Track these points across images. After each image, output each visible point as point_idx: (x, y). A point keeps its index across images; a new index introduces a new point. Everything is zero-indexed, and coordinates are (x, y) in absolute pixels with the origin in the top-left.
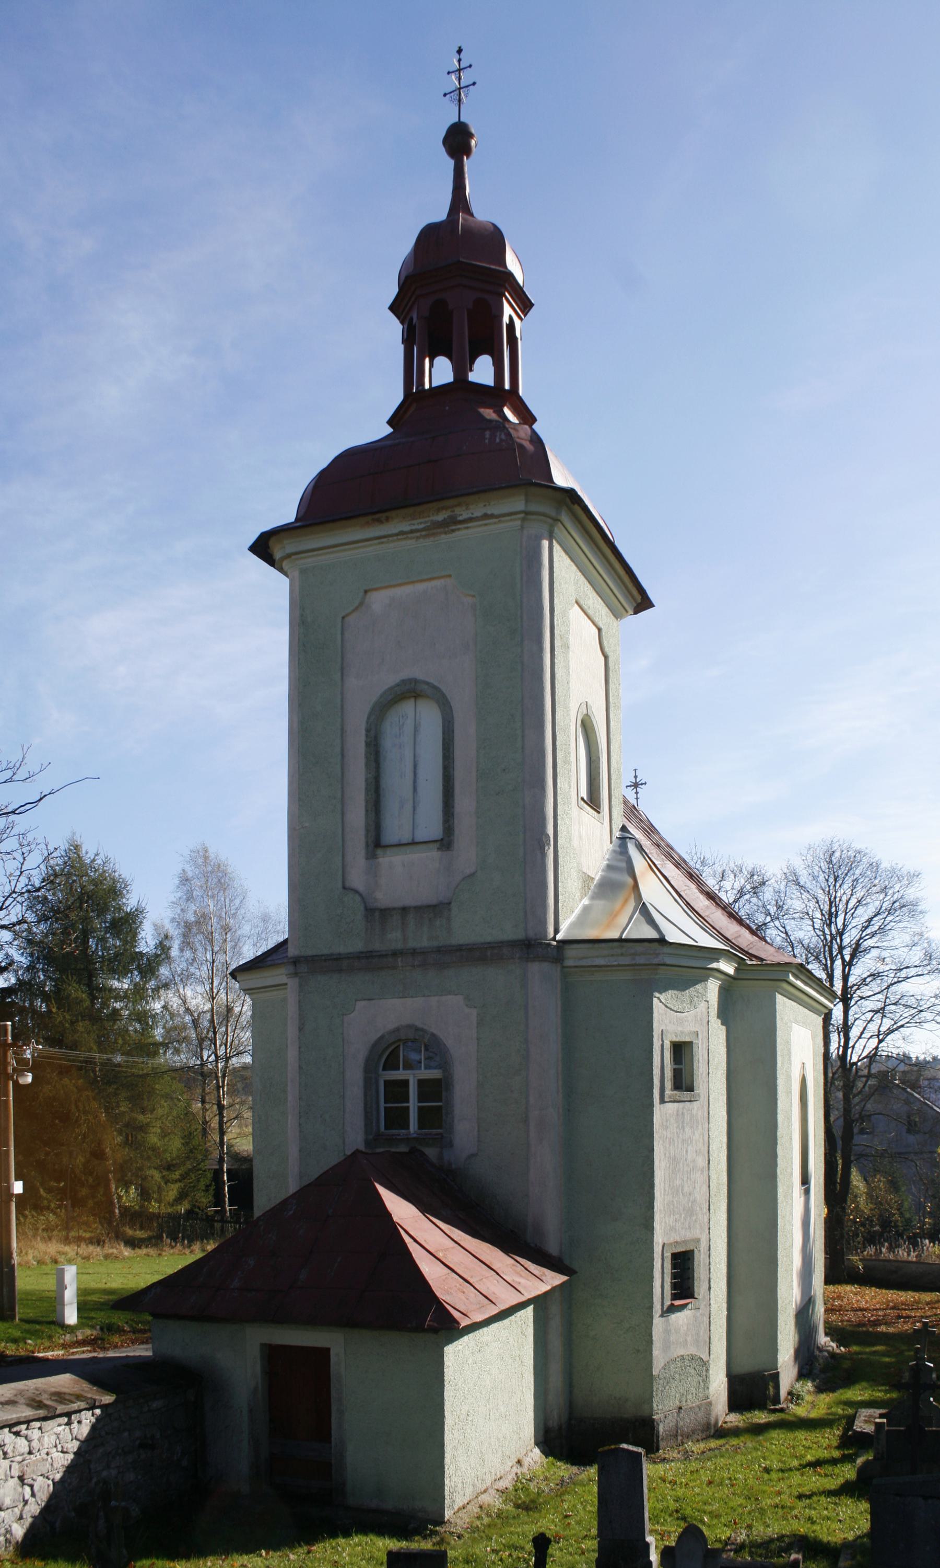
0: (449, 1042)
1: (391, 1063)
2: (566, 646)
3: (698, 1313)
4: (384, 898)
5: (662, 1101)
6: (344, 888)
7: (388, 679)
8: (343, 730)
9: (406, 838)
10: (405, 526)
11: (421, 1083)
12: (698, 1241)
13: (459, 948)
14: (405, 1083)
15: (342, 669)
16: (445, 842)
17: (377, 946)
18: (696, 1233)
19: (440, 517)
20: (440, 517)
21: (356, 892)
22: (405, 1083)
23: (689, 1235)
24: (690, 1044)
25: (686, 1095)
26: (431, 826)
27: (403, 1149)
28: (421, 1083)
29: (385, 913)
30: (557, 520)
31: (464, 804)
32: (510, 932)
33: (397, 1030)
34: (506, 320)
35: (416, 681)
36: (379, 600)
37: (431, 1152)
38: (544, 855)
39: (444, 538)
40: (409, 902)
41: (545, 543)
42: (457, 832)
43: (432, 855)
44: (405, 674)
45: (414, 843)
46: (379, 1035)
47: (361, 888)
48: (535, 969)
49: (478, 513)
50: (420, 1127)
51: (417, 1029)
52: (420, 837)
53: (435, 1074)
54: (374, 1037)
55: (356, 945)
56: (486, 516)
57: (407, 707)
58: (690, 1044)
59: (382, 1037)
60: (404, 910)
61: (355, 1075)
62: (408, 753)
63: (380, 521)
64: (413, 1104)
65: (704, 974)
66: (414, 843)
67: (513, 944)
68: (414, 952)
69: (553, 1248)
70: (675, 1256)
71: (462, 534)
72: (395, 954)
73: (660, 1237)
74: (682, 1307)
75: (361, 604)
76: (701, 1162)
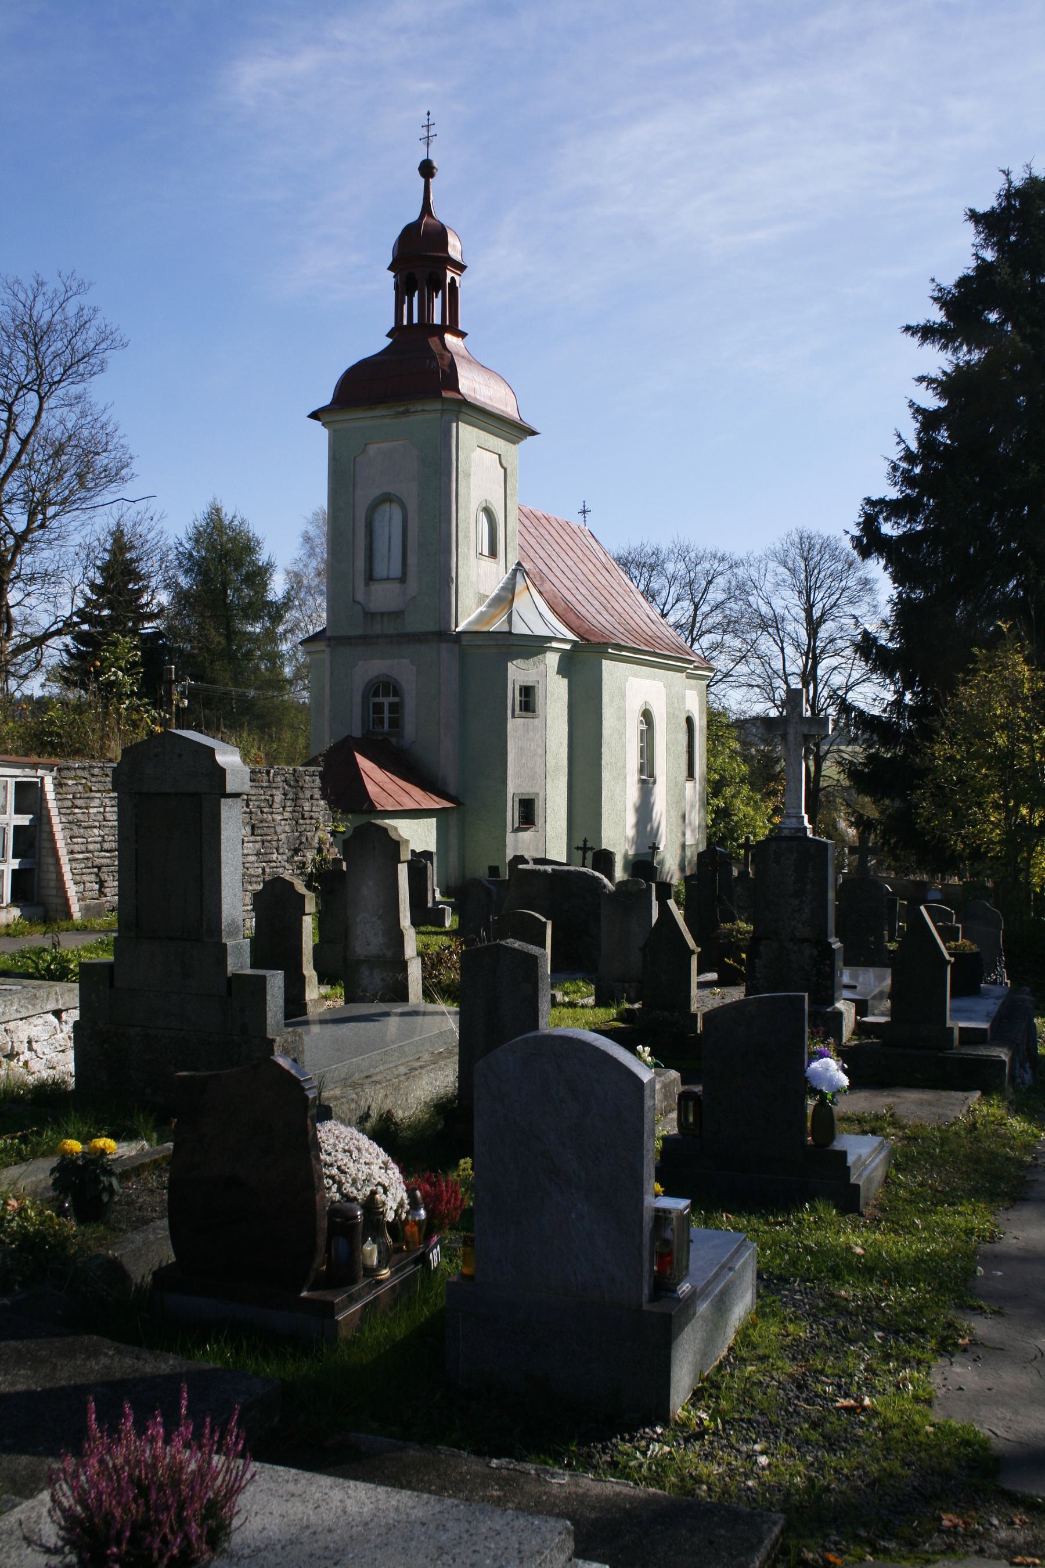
1: (376, 694)
2: (468, 475)
3: (538, 834)
4: (375, 606)
5: (513, 716)
6: (354, 601)
7: (377, 492)
8: (354, 518)
9: (385, 575)
10: (384, 412)
11: (391, 705)
12: (538, 794)
13: (408, 635)
15: (354, 485)
16: (403, 579)
18: (536, 790)
19: (401, 409)
20: (401, 409)
21: (359, 603)
23: (531, 791)
24: (533, 687)
25: (530, 714)
26: (396, 570)
27: (380, 738)
28: (391, 705)
29: (373, 615)
30: (460, 412)
31: (412, 560)
32: (432, 627)
33: (378, 676)
34: (448, 280)
35: (389, 494)
36: (372, 449)
37: (393, 740)
38: (450, 588)
39: (404, 420)
40: (384, 609)
41: (454, 425)
43: (395, 586)
44: (385, 490)
45: (388, 579)
48: (444, 646)
49: (420, 408)
50: (390, 727)
51: (388, 676)
52: (391, 576)
53: (396, 699)
55: (359, 632)
56: (423, 411)
57: (386, 507)
58: (533, 687)
60: (382, 614)
61: (358, 699)
62: (387, 530)
63: (371, 409)
64: (386, 715)
65: (544, 650)
66: (388, 579)
67: (433, 633)
68: (386, 636)
69: (452, 791)
70: (520, 801)
71: (412, 418)
72: (378, 637)
73: (511, 789)
74: (526, 830)
75: (364, 451)
76: (540, 751)
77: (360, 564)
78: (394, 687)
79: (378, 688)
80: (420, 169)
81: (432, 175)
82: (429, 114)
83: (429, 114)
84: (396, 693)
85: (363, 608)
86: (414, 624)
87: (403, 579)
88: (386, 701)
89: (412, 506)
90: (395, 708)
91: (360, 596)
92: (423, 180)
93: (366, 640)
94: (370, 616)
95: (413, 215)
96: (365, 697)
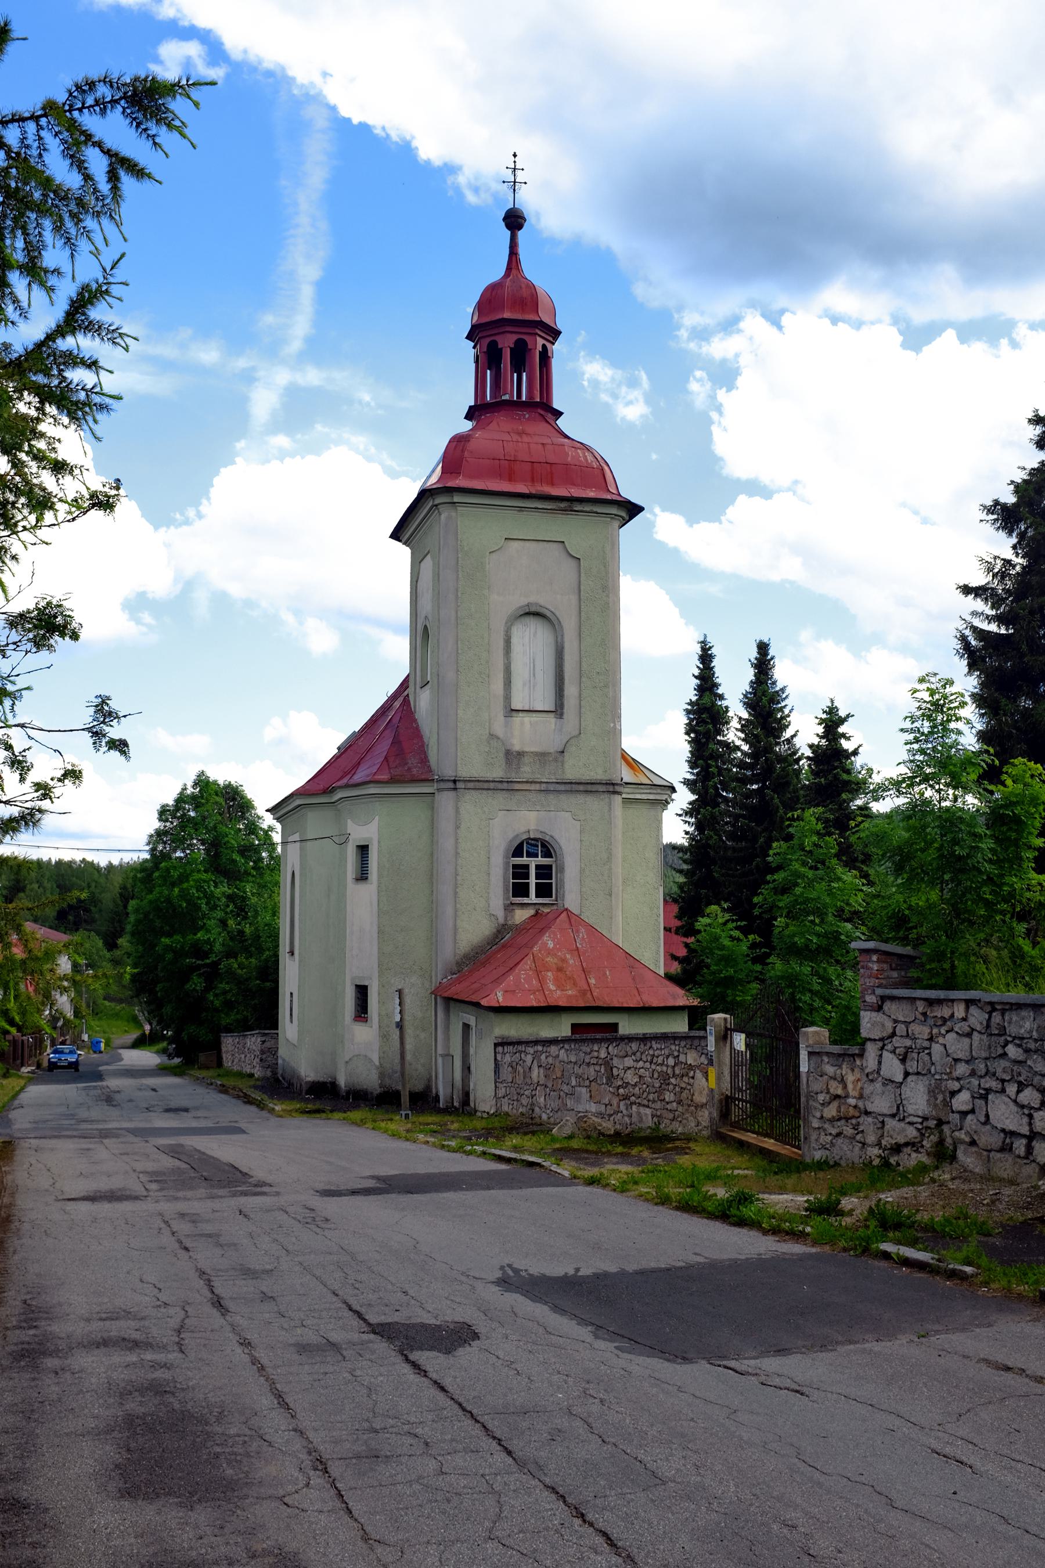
0: (563, 842)
7: (518, 601)
11: (537, 867)
14: (527, 867)
16: (558, 710)
17: (513, 777)
21: (498, 738)
22: (527, 867)
26: (544, 700)
31: (571, 690)
42: (566, 707)
43: (551, 719)
44: (532, 599)
46: (515, 834)
47: (501, 736)
54: (511, 835)
59: (517, 835)
64: (533, 881)
77: (497, 686)
78: (543, 845)
79: (521, 845)
80: (504, 219)
81: (520, 227)
82: (515, 155)
83: (515, 155)
84: (547, 854)
85: (503, 744)
86: (574, 769)
87: (558, 710)
88: (533, 863)
89: (569, 626)
90: (544, 872)
91: (499, 729)
92: (509, 233)
93: (504, 786)
94: (512, 757)
95: (497, 272)
96: (506, 857)
